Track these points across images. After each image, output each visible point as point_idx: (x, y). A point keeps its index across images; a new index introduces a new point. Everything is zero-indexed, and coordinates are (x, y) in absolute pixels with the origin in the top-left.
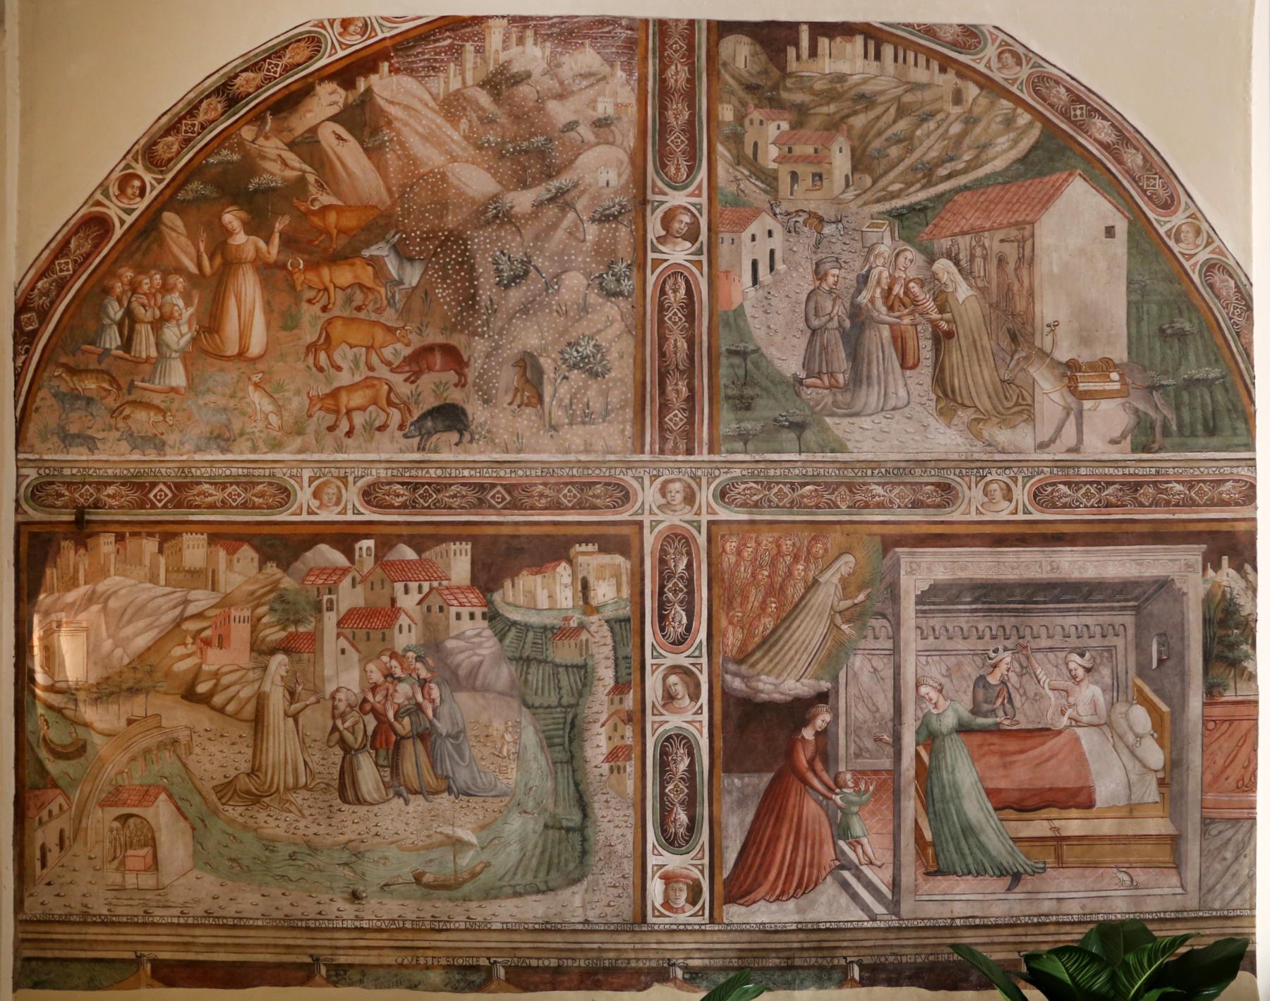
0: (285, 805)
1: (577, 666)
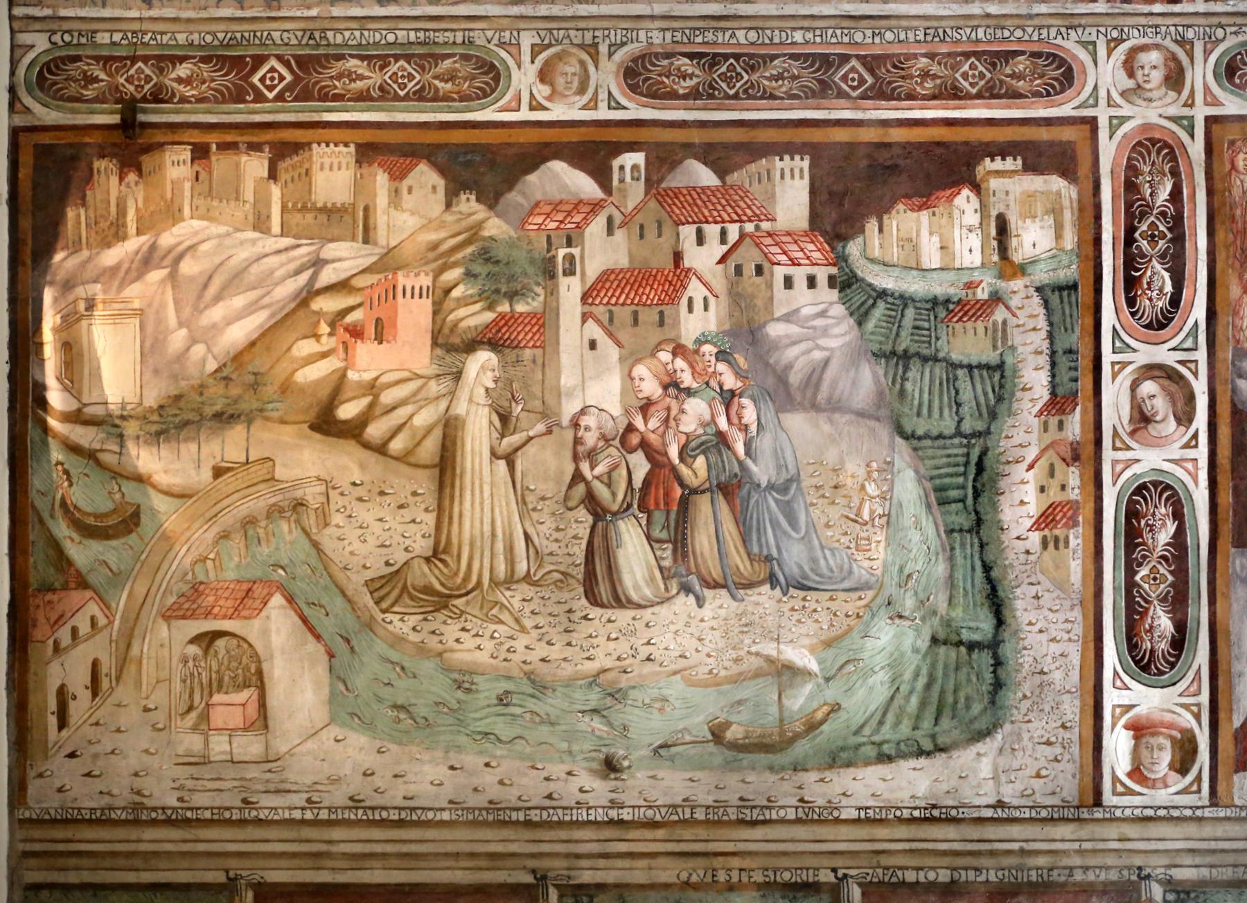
0: (491, 611)
1: (988, 367)
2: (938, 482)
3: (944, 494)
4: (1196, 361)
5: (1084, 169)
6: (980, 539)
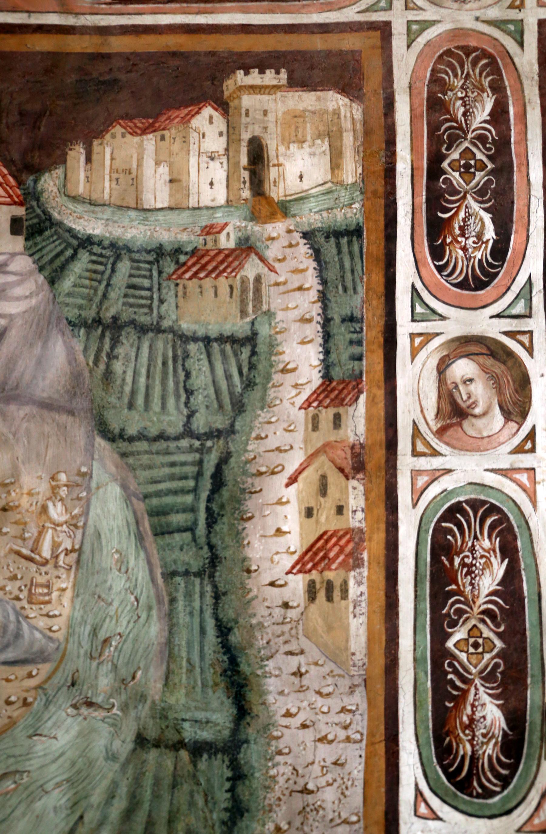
1: (232, 340)
2: (155, 501)
3: (163, 519)
4: (531, 333)
5: (372, 83)
6: (215, 586)
